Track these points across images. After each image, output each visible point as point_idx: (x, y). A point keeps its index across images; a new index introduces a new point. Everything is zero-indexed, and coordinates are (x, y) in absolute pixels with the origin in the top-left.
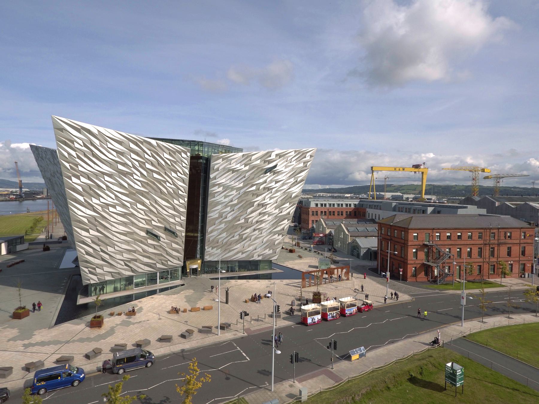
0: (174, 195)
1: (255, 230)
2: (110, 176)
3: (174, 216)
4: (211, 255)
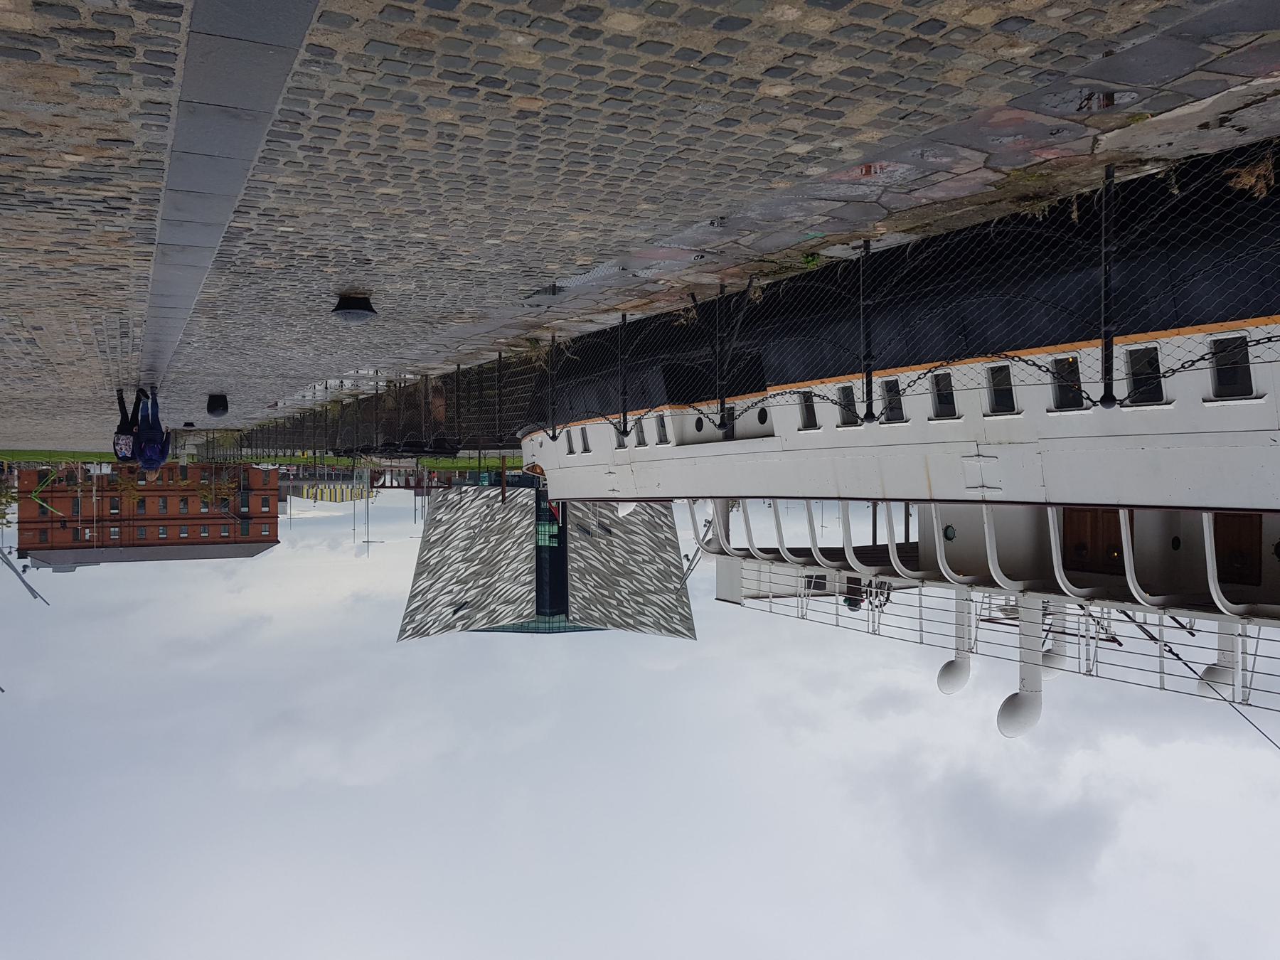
1: (475, 527)
2: (649, 591)
3: (583, 548)
4: (528, 495)
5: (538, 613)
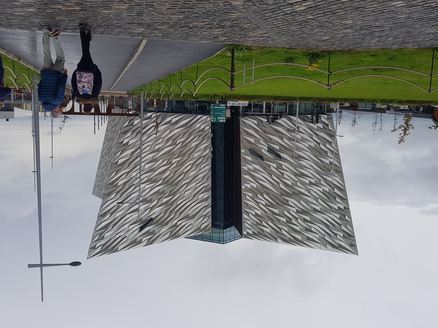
0: (257, 192)
1: (159, 150)
2: (315, 210)
3: (255, 170)
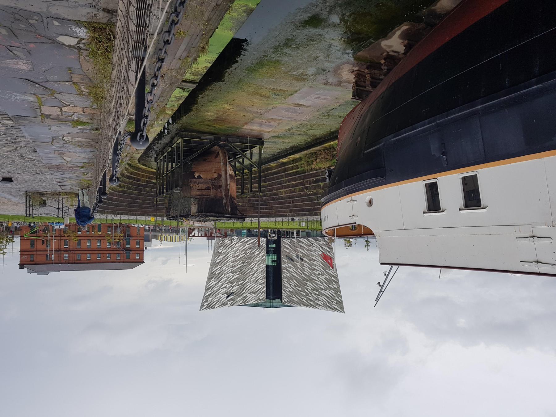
1: (237, 256)
2: (321, 289)
3: (289, 267)
5: (267, 298)
